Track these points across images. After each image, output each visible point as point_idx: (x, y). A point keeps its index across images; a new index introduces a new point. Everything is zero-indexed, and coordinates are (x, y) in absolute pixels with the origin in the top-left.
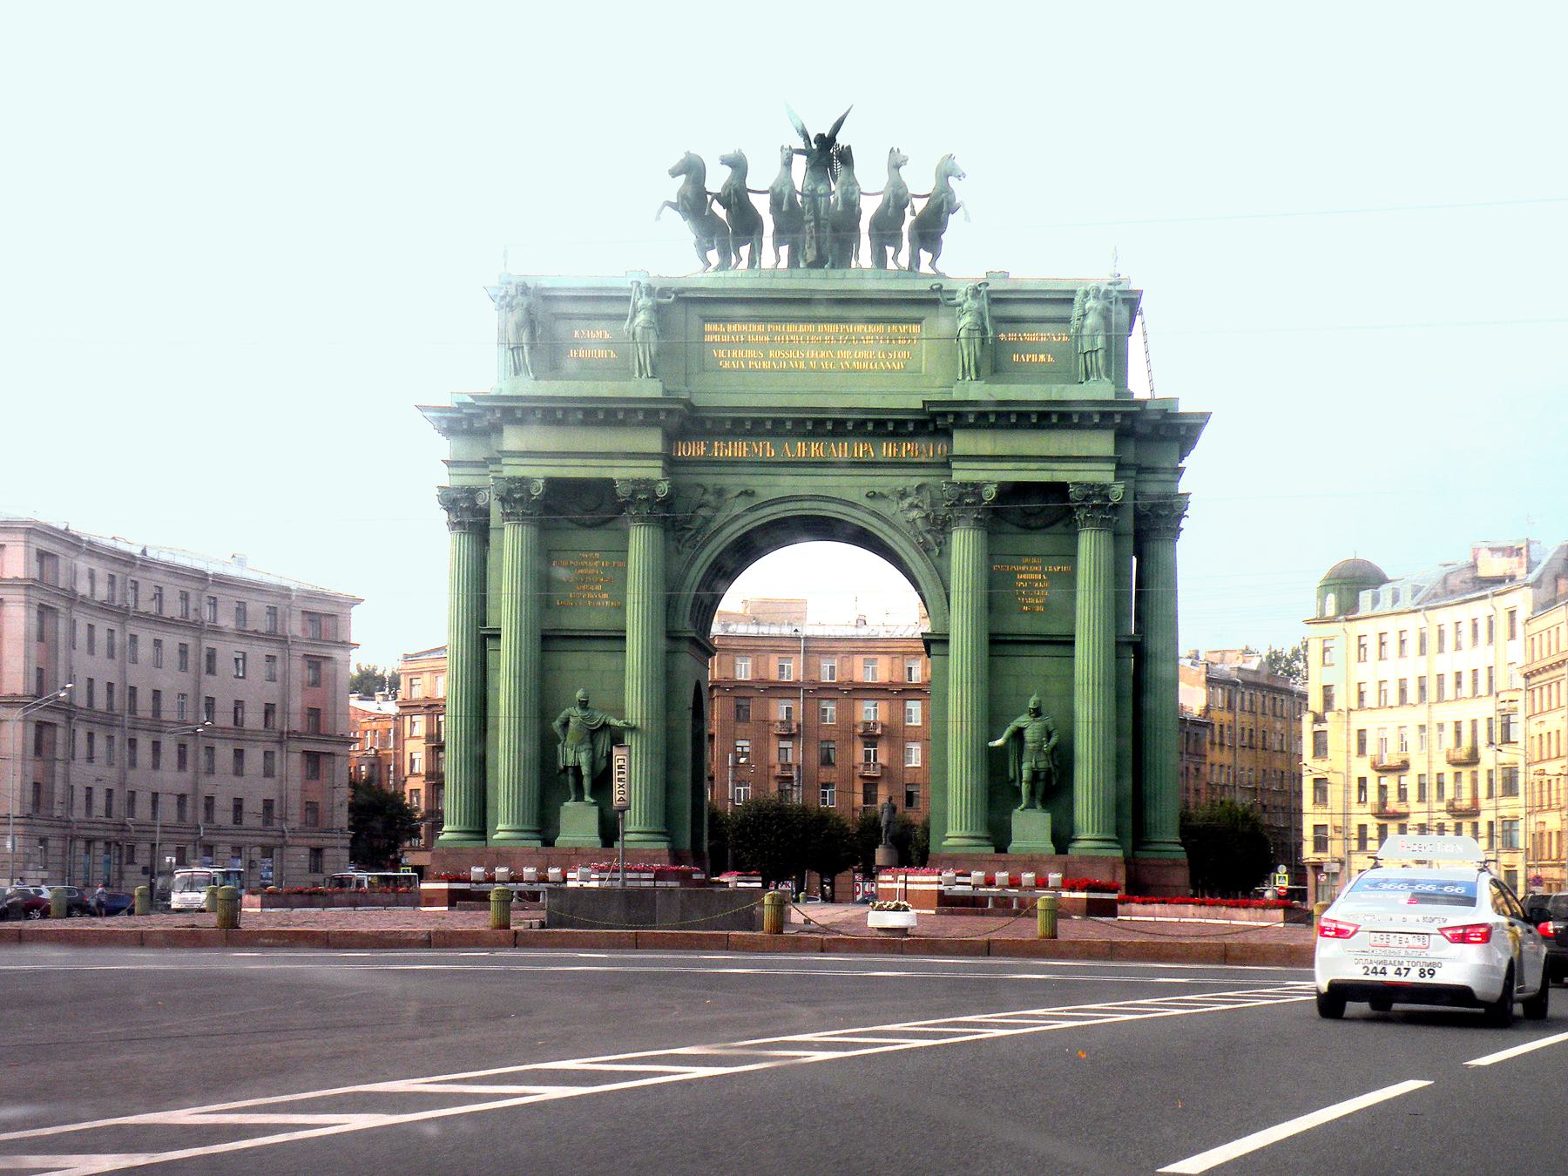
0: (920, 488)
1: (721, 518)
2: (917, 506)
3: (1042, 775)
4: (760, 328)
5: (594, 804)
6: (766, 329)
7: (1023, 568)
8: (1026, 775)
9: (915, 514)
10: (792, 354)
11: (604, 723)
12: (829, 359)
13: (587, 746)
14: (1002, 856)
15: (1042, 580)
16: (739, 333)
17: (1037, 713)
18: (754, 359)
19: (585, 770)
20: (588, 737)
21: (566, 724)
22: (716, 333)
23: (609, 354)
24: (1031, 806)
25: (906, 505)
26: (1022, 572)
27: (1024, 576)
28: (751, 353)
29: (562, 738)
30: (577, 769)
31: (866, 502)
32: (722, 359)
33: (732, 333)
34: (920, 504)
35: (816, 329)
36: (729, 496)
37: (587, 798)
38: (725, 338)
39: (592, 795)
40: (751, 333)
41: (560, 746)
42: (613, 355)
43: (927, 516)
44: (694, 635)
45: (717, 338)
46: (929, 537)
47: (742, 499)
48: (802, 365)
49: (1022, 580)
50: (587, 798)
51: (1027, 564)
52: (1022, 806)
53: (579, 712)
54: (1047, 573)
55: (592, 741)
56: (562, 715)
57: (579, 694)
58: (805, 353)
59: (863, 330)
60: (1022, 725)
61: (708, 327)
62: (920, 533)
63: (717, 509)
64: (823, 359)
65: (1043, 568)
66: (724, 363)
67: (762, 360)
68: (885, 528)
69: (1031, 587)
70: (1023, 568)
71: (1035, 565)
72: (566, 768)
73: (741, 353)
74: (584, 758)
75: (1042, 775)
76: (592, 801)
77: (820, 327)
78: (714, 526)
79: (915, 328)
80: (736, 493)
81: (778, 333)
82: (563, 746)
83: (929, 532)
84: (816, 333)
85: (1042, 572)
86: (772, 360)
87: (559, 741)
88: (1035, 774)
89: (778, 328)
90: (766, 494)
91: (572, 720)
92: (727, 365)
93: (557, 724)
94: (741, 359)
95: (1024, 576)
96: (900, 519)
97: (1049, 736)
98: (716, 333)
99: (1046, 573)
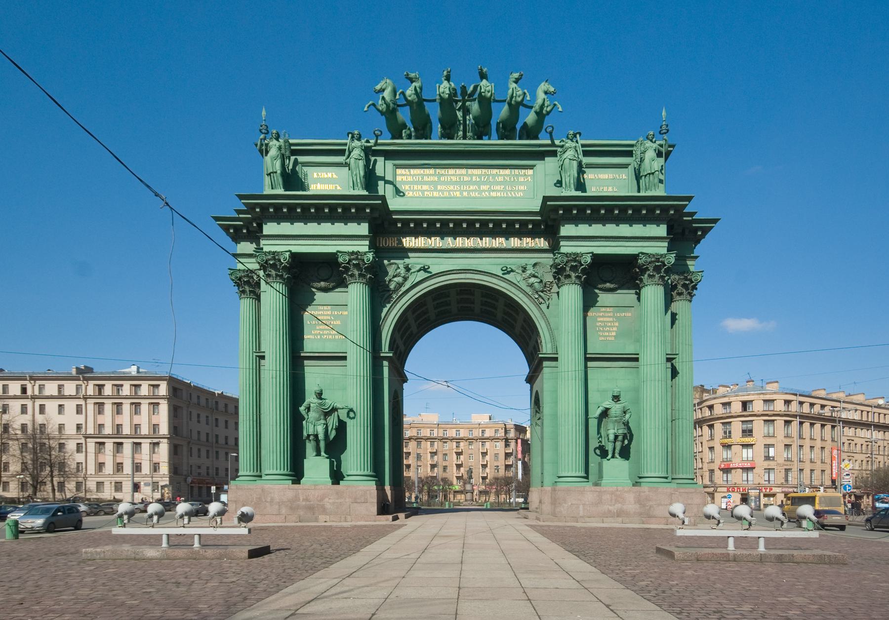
0: (535, 265)
1: (408, 285)
2: (534, 276)
3: (620, 438)
4: (432, 171)
5: (327, 458)
6: (435, 172)
7: (601, 314)
8: (612, 437)
9: (532, 280)
10: (452, 188)
11: (333, 407)
12: (475, 191)
13: (323, 421)
14: (598, 488)
15: (613, 322)
16: (418, 175)
17: (616, 398)
18: (427, 191)
19: (321, 436)
20: (322, 417)
21: (308, 409)
22: (404, 175)
23: (336, 187)
24: (613, 457)
25: (528, 275)
26: (600, 317)
27: (602, 319)
28: (425, 187)
29: (306, 417)
30: (316, 436)
31: (500, 273)
32: (407, 190)
33: (415, 175)
34: (536, 274)
35: (467, 172)
36: (412, 271)
37: (323, 453)
38: (410, 179)
39: (325, 453)
40: (426, 175)
41: (304, 422)
42: (339, 188)
43: (541, 281)
44: (391, 355)
45: (404, 178)
46: (541, 294)
47: (422, 272)
48: (458, 194)
50: (323, 453)
51: (604, 312)
52: (610, 456)
53: (316, 401)
54: (617, 318)
55: (326, 420)
56: (305, 404)
57: (317, 389)
58: (460, 187)
59: (496, 173)
60: (608, 407)
61: (399, 171)
62: (537, 292)
63: (405, 279)
64: (472, 191)
65: (614, 315)
66: (409, 193)
67: (432, 191)
68: (513, 290)
70: (601, 314)
71: (610, 312)
72: (309, 436)
73: (419, 187)
74: (320, 430)
75: (620, 438)
76: (327, 456)
77: (470, 171)
78: (403, 289)
80: (418, 268)
81: (442, 175)
82: (306, 422)
83: (542, 292)
84: (467, 175)
85: (613, 317)
86: (439, 191)
87: (304, 419)
88: (616, 437)
89: (442, 171)
90: (434, 270)
91: (312, 405)
92: (411, 194)
93: (302, 409)
94: (420, 190)
95: (602, 319)
96: (523, 285)
97: (625, 412)
98: (404, 175)
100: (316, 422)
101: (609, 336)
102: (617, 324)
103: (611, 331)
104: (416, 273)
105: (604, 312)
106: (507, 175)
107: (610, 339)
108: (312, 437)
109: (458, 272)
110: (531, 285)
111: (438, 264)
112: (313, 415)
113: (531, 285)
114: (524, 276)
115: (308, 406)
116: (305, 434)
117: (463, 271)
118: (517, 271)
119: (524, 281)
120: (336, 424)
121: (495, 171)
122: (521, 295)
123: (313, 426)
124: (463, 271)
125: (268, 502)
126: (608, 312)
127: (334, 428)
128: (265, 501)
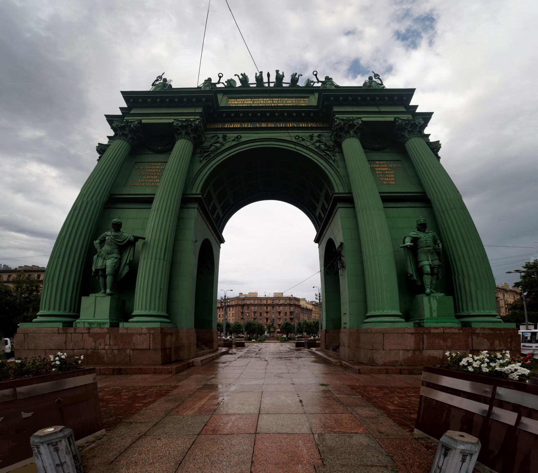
7: (378, 166)
13: (114, 255)
20: (116, 251)
27: (379, 169)
29: (99, 250)
30: (104, 270)
31: (294, 140)
49: (379, 171)
51: (379, 164)
54: (390, 168)
69: (384, 174)
70: (378, 166)
71: (384, 164)
79: (306, 99)
85: (388, 167)
95: (379, 169)
96: (312, 147)
99: (390, 168)
100: (106, 256)
101: (389, 181)
102: (392, 172)
103: (390, 178)
104: (231, 142)
105: (379, 164)
106: (294, 101)
107: (391, 183)
108: (100, 273)
109: (262, 140)
110: (319, 147)
111: (246, 137)
112: (106, 248)
113: (319, 147)
114: (312, 142)
115: (103, 239)
116: (93, 269)
117: (266, 140)
118: (306, 139)
119: (313, 146)
120: (130, 257)
121: (286, 99)
122: (311, 154)
123: (102, 259)
124: (266, 140)
125: (31, 350)
126: (382, 164)
127: (128, 262)
128: (28, 349)
